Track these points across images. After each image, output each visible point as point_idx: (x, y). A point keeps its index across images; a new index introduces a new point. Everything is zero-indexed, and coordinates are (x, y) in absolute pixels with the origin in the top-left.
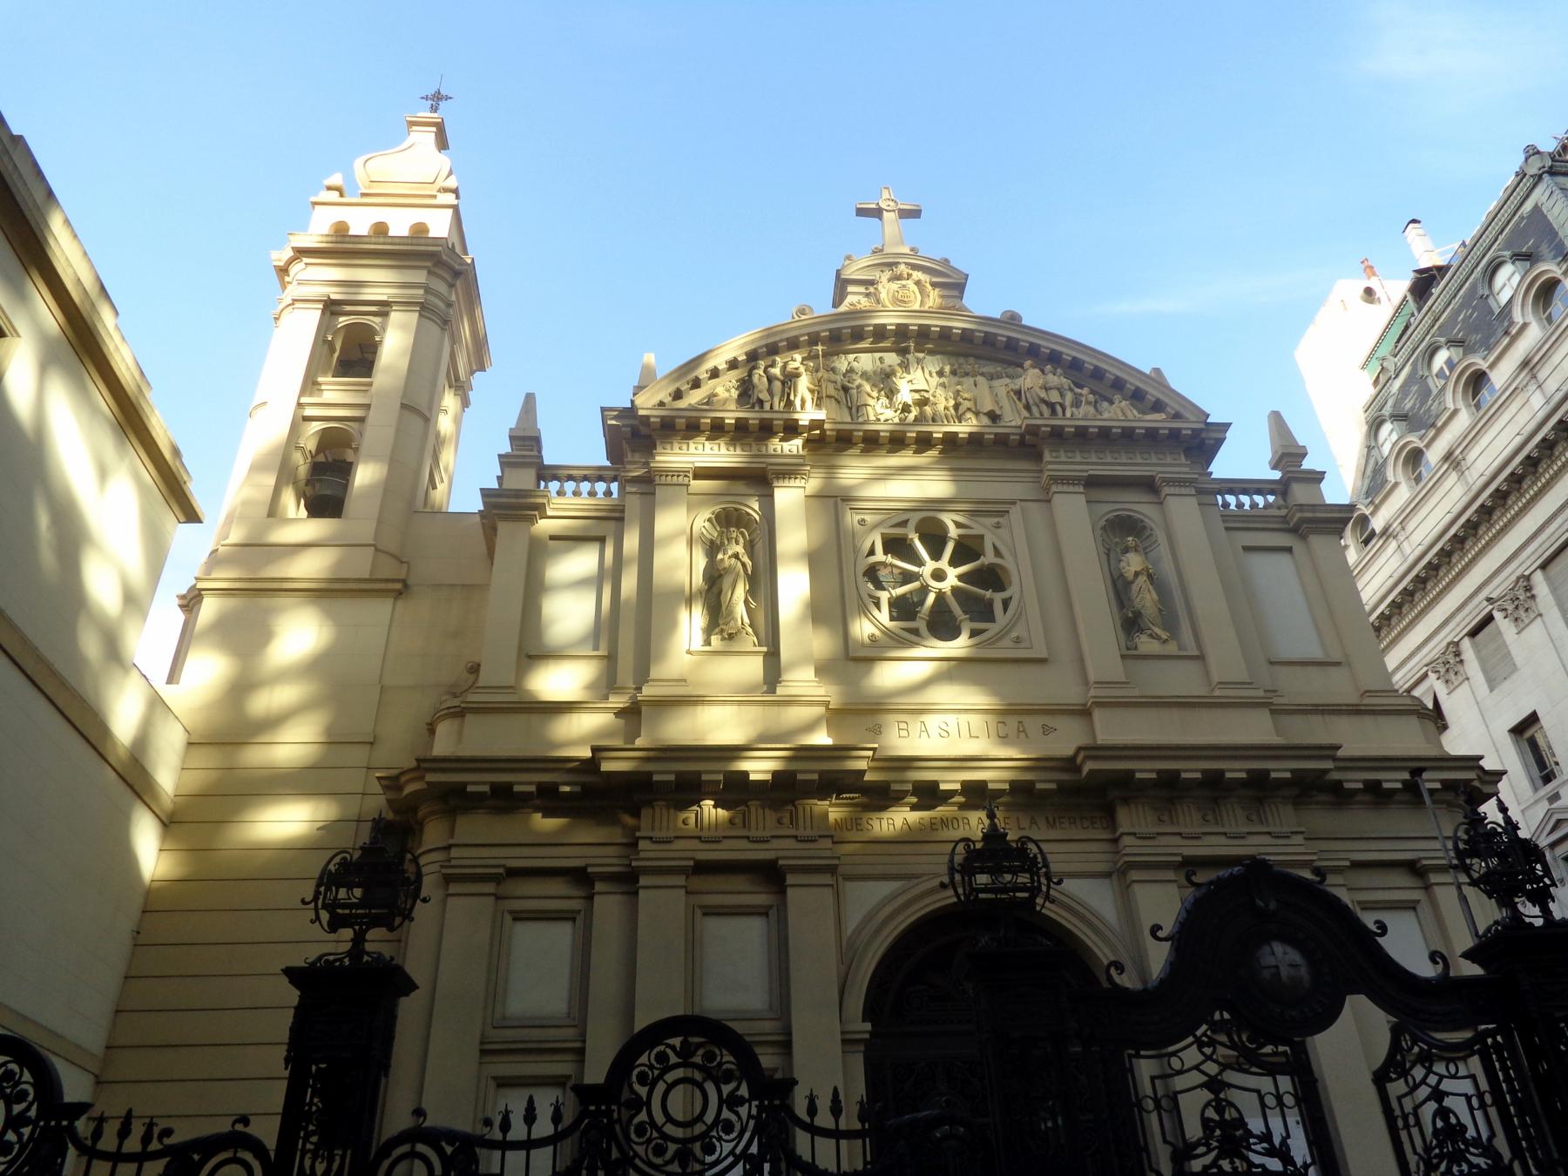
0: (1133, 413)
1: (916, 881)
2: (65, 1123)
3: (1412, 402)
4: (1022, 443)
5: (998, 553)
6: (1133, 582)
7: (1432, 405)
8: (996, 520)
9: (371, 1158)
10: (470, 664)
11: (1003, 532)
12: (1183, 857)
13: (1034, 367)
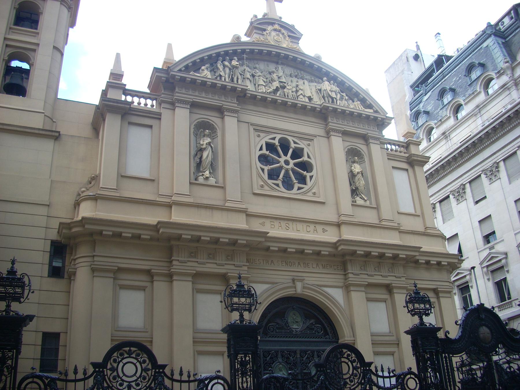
0: (361, 107)
1: (275, 285)
2: (101, 370)
3: (431, 107)
4: (320, 112)
5: (309, 157)
6: (356, 176)
7: (439, 111)
8: (309, 142)
9: (230, 383)
10: (93, 175)
11: (310, 148)
12: (368, 283)
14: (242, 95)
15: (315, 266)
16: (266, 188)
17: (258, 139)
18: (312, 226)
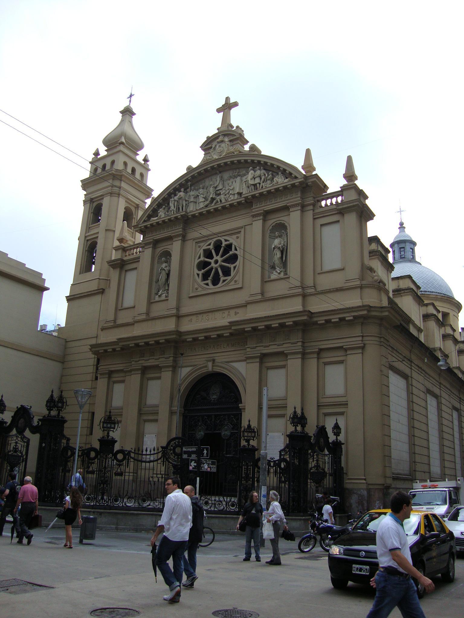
13: (251, 170)
16: (200, 289)
17: (198, 249)
18: (226, 312)
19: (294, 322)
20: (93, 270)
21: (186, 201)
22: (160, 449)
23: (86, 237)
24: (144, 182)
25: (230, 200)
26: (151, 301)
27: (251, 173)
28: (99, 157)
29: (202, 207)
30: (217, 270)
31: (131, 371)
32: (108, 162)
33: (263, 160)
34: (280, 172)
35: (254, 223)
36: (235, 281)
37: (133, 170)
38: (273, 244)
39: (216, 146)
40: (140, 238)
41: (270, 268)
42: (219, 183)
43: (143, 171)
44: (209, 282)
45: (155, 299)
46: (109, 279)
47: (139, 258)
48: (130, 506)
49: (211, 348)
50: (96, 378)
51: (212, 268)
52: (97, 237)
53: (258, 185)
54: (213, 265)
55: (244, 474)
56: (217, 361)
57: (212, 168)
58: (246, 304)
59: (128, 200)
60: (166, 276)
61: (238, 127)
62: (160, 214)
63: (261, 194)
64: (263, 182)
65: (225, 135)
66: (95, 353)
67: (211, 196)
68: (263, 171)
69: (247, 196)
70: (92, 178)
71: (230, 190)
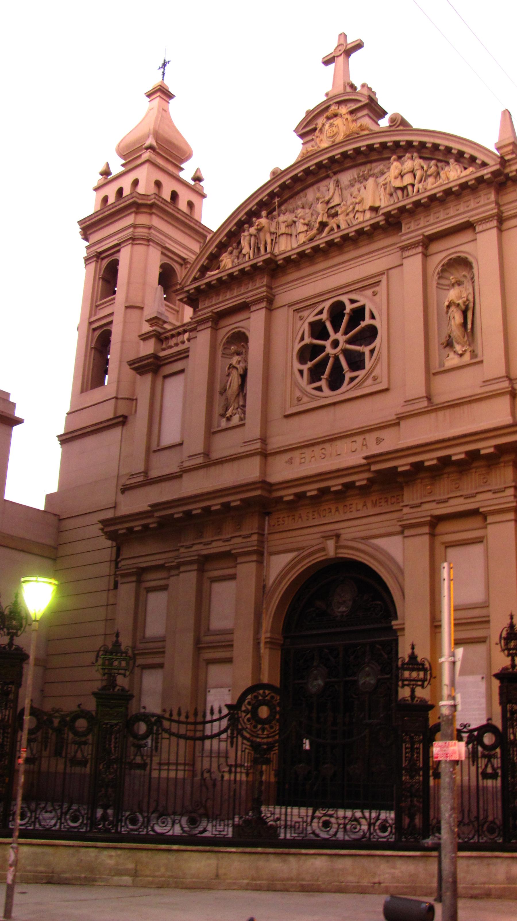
1: (302, 551)
5: (373, 317)
11: (377, 298)
13: (395, 160)
14: (273, 266)
15: (360, 507)
16: (305, 399)
18: (359, 439)
19: (496, 447)
20: (106, 384)
21: (272, 233)
22: (225, 711)
23: (91, 323)
24: (196, 217)
25: (355, 223)
26: (213, 430)
27: (395, 167)
28: (109, 177)
29: (304, 242)
30: (336, 359)
31: (178, 567)
32: (126, 183)
33: (416, 139)
34: (451, 158)
35: (405, 262)
36: (374, 377)
37: (174, 195)
38: (447, 300)
39: (323, 125)
40: (188, 312)
41: (442, 346)
42: (334, 194)
43: (194, 198)
44: (323, 383)
45: (219, 426)
46: (135, 398)
47: (188, 351)
48: (162, 834)
49: (330, 512)
50: (116, 587)
51: (327, 357)
52: (111, 323)
53: (410, 188)
54: (329, 350)
55: (406, 760)
56: (343, 537)
57: (319, 165)
58: (397, 421)
59: (165, 251)
60: (240, 380)
61: (363, 86)
62: (223, 263)
63: (417, 204)
64: (420, 181)
65: (339, 103)
66: (111, 536)
67: (319, 219)
68: (418, 162)
69: (390, 212)
70: (97, 216)
71: (356, 203)
